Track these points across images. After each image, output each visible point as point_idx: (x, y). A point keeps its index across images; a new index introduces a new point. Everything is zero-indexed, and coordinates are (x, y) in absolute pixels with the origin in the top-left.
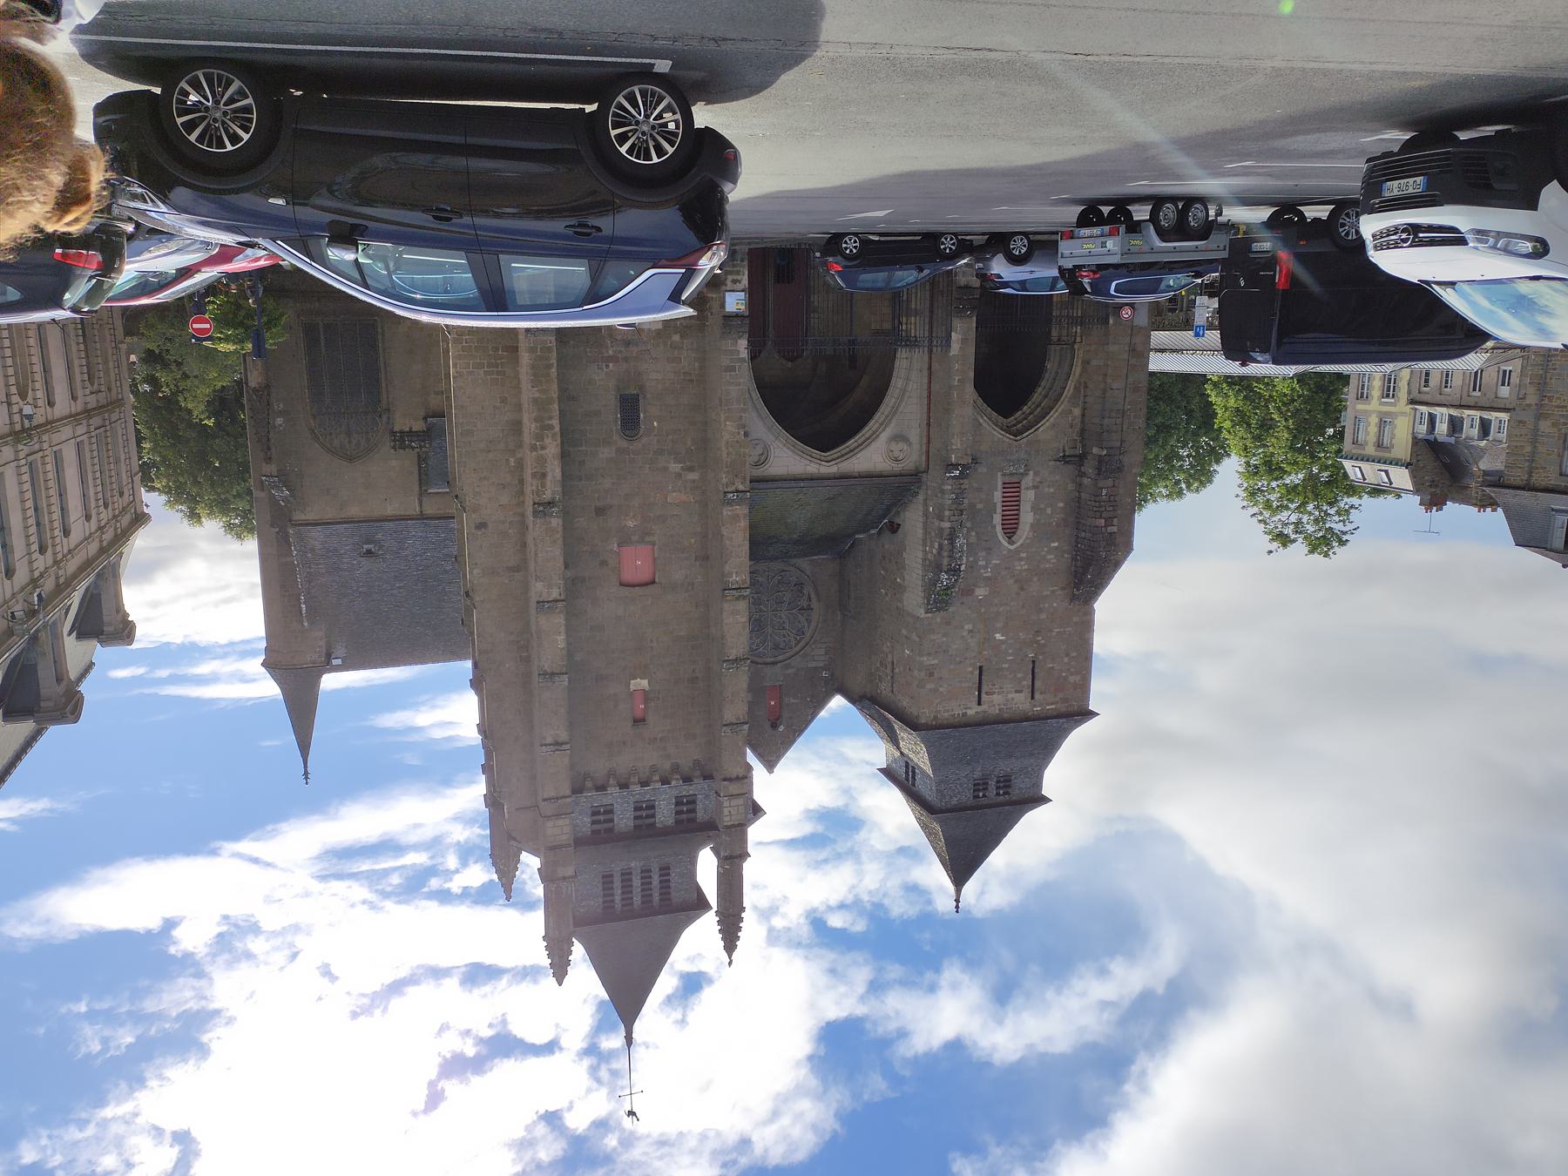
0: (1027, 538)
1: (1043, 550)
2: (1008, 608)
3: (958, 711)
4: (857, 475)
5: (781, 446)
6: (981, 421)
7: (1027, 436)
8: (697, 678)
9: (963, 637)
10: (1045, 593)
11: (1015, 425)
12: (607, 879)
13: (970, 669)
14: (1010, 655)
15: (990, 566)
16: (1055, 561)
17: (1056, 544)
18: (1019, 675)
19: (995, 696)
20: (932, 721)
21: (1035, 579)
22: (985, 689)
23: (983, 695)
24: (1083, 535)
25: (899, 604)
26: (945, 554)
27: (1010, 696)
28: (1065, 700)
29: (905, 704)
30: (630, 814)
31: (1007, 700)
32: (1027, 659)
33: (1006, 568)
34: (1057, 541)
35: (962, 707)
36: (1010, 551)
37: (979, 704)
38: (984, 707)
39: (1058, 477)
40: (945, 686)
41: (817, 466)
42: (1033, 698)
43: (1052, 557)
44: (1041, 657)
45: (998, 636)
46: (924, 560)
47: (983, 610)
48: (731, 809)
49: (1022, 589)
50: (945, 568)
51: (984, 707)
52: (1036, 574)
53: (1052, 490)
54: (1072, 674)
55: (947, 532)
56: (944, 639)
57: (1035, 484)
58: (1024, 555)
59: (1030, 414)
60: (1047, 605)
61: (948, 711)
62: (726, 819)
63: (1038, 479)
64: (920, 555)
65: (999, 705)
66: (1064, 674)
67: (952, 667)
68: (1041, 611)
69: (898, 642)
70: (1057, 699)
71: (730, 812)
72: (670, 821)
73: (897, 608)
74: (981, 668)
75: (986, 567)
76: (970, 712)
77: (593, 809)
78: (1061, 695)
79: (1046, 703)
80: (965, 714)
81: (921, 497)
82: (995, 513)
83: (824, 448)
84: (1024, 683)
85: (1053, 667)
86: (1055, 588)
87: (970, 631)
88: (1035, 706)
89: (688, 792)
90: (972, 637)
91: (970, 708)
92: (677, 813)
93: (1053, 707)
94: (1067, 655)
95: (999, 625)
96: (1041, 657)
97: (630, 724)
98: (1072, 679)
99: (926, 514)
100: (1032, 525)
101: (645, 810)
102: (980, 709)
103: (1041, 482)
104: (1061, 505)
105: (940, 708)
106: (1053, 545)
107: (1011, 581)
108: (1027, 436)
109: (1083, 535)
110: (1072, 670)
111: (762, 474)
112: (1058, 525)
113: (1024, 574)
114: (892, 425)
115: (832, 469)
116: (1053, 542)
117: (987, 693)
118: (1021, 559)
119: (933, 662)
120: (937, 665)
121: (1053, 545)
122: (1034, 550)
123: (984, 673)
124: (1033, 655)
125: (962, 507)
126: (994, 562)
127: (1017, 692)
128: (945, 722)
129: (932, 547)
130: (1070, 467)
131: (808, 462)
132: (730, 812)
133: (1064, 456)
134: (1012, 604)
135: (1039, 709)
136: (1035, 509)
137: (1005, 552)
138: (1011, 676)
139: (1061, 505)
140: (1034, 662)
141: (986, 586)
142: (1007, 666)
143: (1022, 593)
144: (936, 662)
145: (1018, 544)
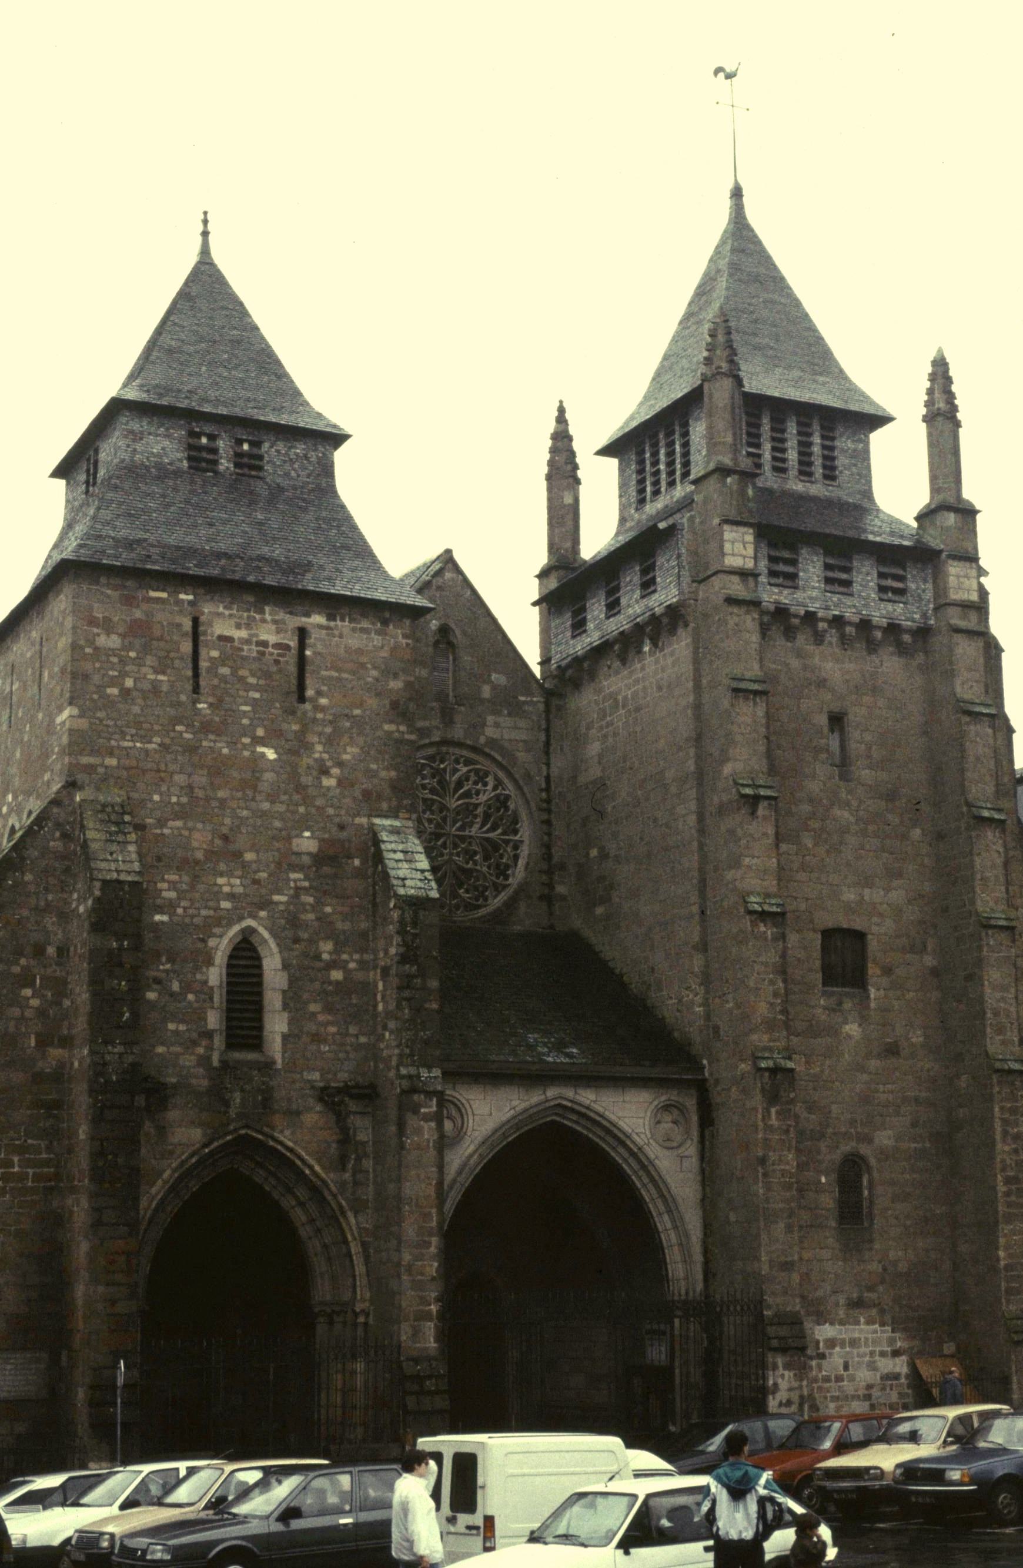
0: (221, 936)
1: (185, 908)
2: (253, 805)
3: (343, 625)
9: (340, 764)
10: (179, 823)
12: (830, 474)
13: (323, 701)
17: (158, 918)
18: (225, 671)
21: (199, 855)
23: (293, 643)
27: (243, 634)
30: (857, 578)
31: (248, 626)
32: (211, 700)
34: (157, 924)
35: (336, 632)
36: (254, 917)
37: (302, 633)
40: (370, 679)
41: (578, 1097)
42: (196, 621)
43: (165, 894)
44: (183, 698)
45: (271, 754)
49: (225, 838)
52: (197, 862)
53: (171, 1026)
54: (113, 652)
58: (226, 905)
60: (174, 799)
61: (363, 630)
65: (264, 621)
66: (132, 654)
67: (357, 712)
70: (145, 606)
71: (745, 548)
72: (804, 552)
74: (302, 699)
77: (903, 600)
78: (138, 614)
80: (331, 617)
82: (284, 992)
83: (554, 1126)
84: (215, 654)
85: (156, 672)
86: (158, 831)
87: (325, 772)
88: (190, 602)
89: (781, 593)
90: (321, 761)
91: (320, 627)
92: (794, 562)
93: (153, 594)
94: (126, 693)
96: (183, 698)
97: (851, 717)
98: (113, 641)
104: (151, 996)
105: (377, 640)
106: (165, 918)
107: (249, 856)
110: (115, 660)
115: (552, 1092)
117: (287, 647)
118: (231, 896)
121: (165, 918)
122: (204, 912)
123: (294, 688)
124: (200, 706)
126: (283, 899)
127: (229, 639)
132: (745, 548)
134: (245, 813)
135: (182, 596)
137: (263, 914)
138: (241, 673)
139: (151, 996)
140: (196, 689)
143: (225, 830)
145: (236, 928)
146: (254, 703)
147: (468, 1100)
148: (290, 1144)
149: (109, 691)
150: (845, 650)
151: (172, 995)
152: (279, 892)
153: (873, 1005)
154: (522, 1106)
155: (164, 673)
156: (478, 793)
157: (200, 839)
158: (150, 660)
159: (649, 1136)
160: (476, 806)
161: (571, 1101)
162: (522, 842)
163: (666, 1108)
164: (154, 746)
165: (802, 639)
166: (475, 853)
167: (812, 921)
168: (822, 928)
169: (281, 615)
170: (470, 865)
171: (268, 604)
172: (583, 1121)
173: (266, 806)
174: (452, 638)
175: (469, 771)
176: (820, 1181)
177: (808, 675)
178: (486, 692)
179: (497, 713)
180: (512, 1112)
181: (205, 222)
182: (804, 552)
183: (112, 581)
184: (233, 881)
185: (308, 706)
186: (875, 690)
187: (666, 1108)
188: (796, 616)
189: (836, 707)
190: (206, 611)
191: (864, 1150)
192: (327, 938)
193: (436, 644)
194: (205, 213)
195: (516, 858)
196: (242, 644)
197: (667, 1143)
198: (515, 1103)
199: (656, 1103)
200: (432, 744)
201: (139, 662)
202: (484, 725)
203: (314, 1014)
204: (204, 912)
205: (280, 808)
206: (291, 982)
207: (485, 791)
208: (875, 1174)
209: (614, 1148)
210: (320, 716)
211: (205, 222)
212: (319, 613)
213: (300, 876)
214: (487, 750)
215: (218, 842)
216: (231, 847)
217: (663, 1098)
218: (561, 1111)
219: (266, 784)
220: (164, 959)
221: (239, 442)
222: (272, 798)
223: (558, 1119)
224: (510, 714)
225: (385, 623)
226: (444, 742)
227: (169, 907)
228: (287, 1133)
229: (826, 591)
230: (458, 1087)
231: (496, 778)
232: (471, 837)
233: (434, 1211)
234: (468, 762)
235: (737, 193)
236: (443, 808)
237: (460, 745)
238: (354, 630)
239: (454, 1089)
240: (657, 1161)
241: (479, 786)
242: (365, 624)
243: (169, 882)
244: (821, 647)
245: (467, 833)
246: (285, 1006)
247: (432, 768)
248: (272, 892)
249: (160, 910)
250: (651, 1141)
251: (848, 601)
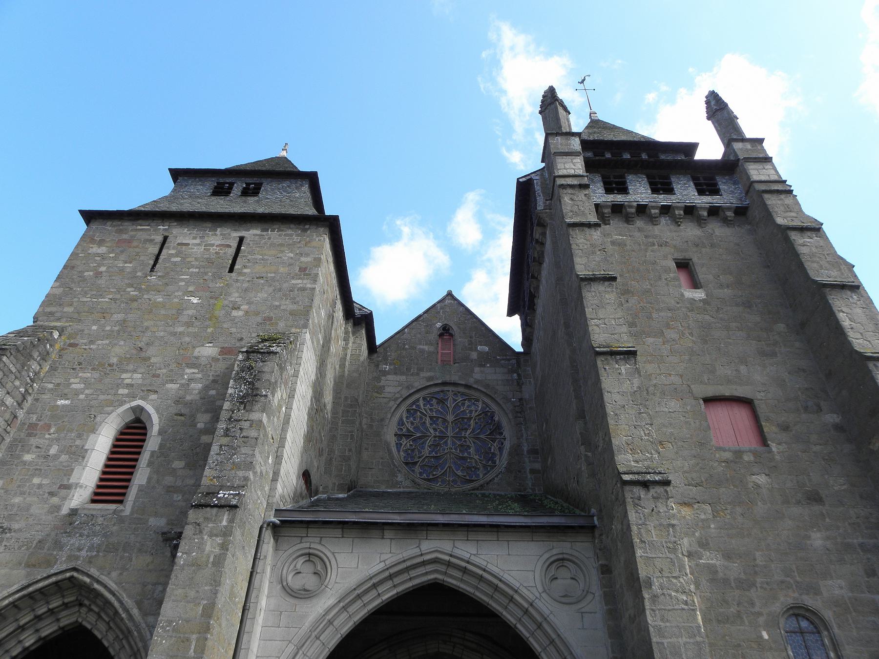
0: (109, 414)
2: (168, 329)
4: (388, 534)
5: (525, 592)
6: (135, 612)
7: (49, 577)
9: (249, 303)
11: (66, 606)
13: (245, 271)
14: (183, 280)
15: (183, 381)
16: (72, 380)
17: (60, 402)
20: (309, 228)
21: (114, 360)
22: (231, 251)
23: (234, 245)
24: (9, 401)
28: (120, 232)
32: (159, 274)
33: (158, 376)
34: (58, 406)
37: (241, 240)
38: (236, 235)
39: (17, 500)
41: (458, 552)
43: (74, 386)
47: (209, 330)
48: (574, 167)
53: (36, 481)
56: (277, 303)
57: (63, 492)
59: (22, 628)
60: (108, 328)
63: (55, 500)
65: (216, 235)
74: (231, 270)
75: (190, 380)
80: (263, 230)
90: (235, 302)
94: (98, 274)
98: (103, 250)
100: (93, 430)
101: (661, 186)
103: (51, 494)
106: (67, 402)
107: (153, 360)
108: (49, 577)
109: (9, 401)
111: (555, 544)
112: (49, 427)
113: (131, 367)
116: (63, 406)
117: (229, 246)
119: (300, 281)
120: (293, 278)
122: (102, 397)
125: (225, 440)
128: (292, 226)
131: (474, 559)
134: (162, 334)
137: (153, 397)
139: (28, 457)
141: (197, 358)
144: (293, 282)
146: (191, 274)
147: (333, 553)
148: (113, 585)
149: (86, 274)
150: (679, 225)
151: (47, 457)
152: (172, 381)
153: (778, 457)
154: (391, 559)
155: (130, 263)
156: (471, 412)
157: (120, 349)
158: (123, 257)
159: (541, 589)
160: (470, 419)
161: (451, 556)
162: (505, 439)
163: (561, 561)
164: (107, 300)
165: (639, 223)
166: (469, 447)
167: (691, 392)
169: (226, 231)
170: (466, 455)
171: (219, 227)
172: (466, 578)
173: (181, 329)
174: (450, 332)
175: (465, 400)
176: (761, 637)
177: (651, 240)
178: (474, 355)
179: (481, 366)
180: (382, 565)
182: (630, 178)
183: (114, 224)
184: (136, 376)
185: (233, 274)
186: (712, 246)
187: (561, 561)
189: (680, 256)
190: (174, 232)
191: (809, 601)
192: (206, 411)
193: (441, 335)
195: (501, 449)
196: (194, 246)
197: (566, 599)
198: (384, 557)
199: (546, 556)
200: (436, 385)
201: (115, 258)
202: (472, 371)
203: (174, 469)
204: (102, 397)
206: (161, 446)
207: (476, 411)
208: (836, 630)
209: (506, 608)
210: (241, 278)
212: (256, 229)
213: (196, 371)
214: (475, 386)
215: (134, 352)
216: (143, 355)
217: (555, 552)
218: (443, 568)
219: (185, 316)
220: (52, 431)
223: (440, 577)
224: (490, 367)
225: (305, 230)
226: (444, 384)
227: (77, 393)
228: (114, 574)
229: (652, 194)
230: (324, 541)
231: (484, 402)
232: (465, 438)
233: (194, 637)
234: (463, 394)
236: (445, 420)
237: (455, 384)
238: (280, 235)
239: (320, 543)
240: (551, 617)
241: (473, 408)
242: (290, 232)
243: (81, 377)
244: (658, 226)
245: (463, 435)
246: (150, 464)
247: (436, 398)
248: (167, 382)
249: (64, 396)
250: (544, 595)
251: (673, 197)
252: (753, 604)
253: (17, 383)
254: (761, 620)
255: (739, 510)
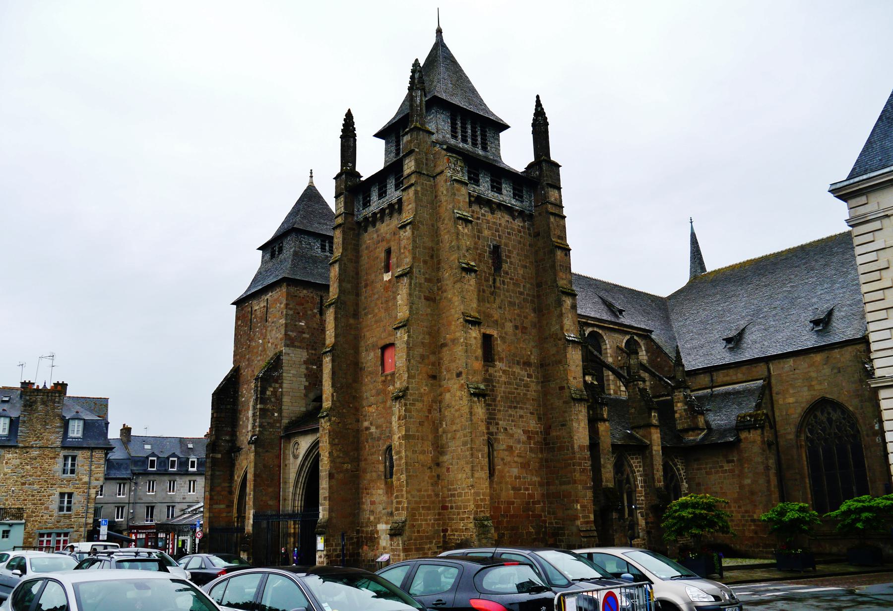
8: (365, 288)
19: (262, 305)
22: (265, 308)
23: (266, 305)
25: (313, 352)
26: (259, 389)
29: (305, 291)
46: (282, 383)
50: (259, 380)
51: (266, 298)
55: (259, 402)
62: (342, 199)
64: (285, 385)
68: (248, 360)
69: (314, 328)
73: (315, 350)
76: (270, 294)
79: (258, 306)
81: (285, 421)
87: (269, 342)
95: (260, 348)
99: (280, 411)
102: (268, 296)
114: (298, 465)
129: (274, 393)
130: (238, 445)
133: (239, 451)
136: (248, 419)
142: (259, 325)
168: (380, 347)
173: (259, 358)
181: (311, 173)
188: (370, 217)
194: (311, 170)
205: (262, 357)
211: (311, 173)
221: (280, 244)
222: (261, 355)
235: (439, 32)
252: (379, 446)
253: (228, 400)
254: (381, 452)
255: (382, 406)
